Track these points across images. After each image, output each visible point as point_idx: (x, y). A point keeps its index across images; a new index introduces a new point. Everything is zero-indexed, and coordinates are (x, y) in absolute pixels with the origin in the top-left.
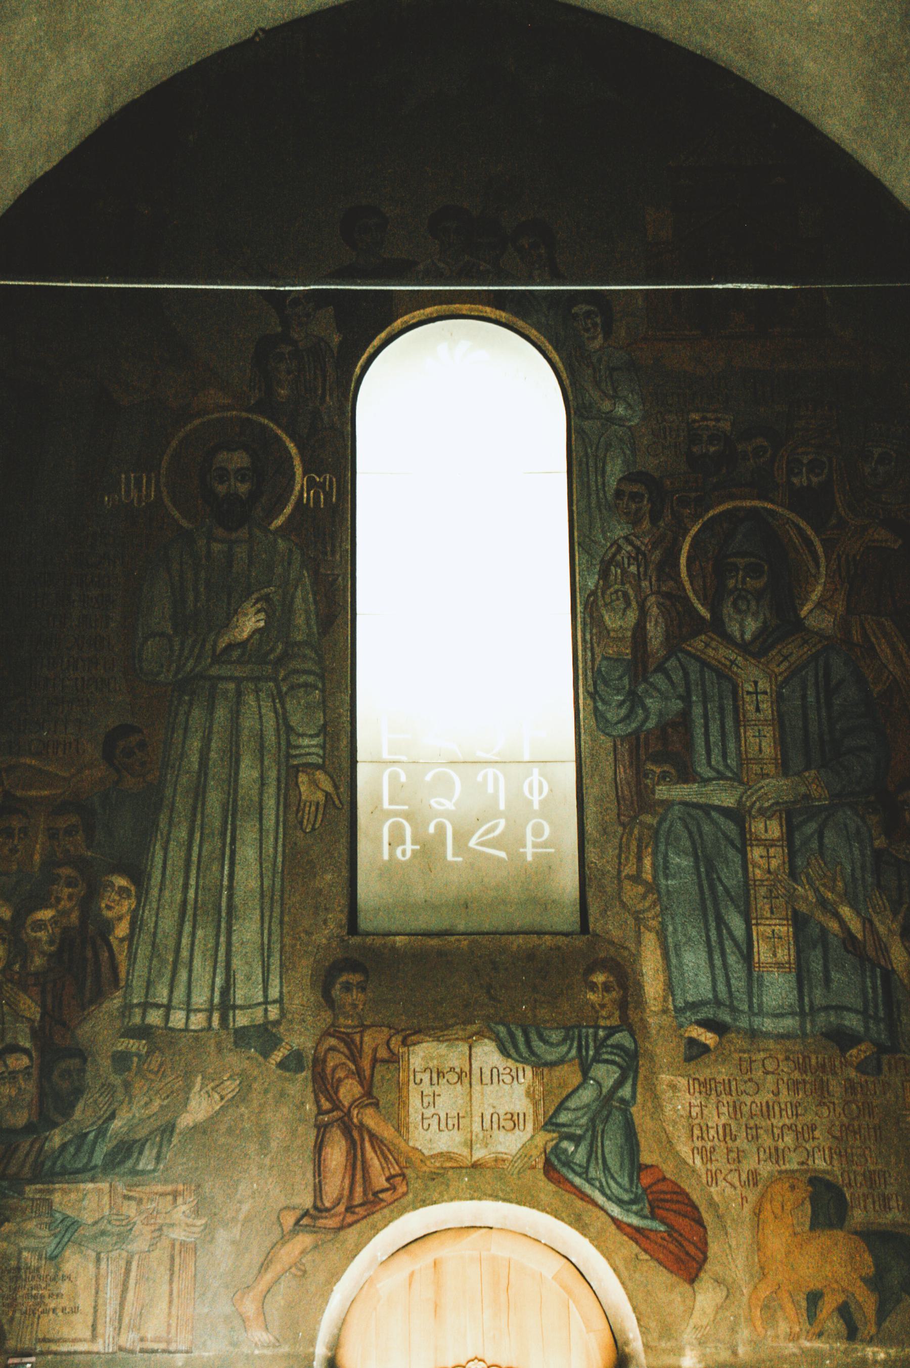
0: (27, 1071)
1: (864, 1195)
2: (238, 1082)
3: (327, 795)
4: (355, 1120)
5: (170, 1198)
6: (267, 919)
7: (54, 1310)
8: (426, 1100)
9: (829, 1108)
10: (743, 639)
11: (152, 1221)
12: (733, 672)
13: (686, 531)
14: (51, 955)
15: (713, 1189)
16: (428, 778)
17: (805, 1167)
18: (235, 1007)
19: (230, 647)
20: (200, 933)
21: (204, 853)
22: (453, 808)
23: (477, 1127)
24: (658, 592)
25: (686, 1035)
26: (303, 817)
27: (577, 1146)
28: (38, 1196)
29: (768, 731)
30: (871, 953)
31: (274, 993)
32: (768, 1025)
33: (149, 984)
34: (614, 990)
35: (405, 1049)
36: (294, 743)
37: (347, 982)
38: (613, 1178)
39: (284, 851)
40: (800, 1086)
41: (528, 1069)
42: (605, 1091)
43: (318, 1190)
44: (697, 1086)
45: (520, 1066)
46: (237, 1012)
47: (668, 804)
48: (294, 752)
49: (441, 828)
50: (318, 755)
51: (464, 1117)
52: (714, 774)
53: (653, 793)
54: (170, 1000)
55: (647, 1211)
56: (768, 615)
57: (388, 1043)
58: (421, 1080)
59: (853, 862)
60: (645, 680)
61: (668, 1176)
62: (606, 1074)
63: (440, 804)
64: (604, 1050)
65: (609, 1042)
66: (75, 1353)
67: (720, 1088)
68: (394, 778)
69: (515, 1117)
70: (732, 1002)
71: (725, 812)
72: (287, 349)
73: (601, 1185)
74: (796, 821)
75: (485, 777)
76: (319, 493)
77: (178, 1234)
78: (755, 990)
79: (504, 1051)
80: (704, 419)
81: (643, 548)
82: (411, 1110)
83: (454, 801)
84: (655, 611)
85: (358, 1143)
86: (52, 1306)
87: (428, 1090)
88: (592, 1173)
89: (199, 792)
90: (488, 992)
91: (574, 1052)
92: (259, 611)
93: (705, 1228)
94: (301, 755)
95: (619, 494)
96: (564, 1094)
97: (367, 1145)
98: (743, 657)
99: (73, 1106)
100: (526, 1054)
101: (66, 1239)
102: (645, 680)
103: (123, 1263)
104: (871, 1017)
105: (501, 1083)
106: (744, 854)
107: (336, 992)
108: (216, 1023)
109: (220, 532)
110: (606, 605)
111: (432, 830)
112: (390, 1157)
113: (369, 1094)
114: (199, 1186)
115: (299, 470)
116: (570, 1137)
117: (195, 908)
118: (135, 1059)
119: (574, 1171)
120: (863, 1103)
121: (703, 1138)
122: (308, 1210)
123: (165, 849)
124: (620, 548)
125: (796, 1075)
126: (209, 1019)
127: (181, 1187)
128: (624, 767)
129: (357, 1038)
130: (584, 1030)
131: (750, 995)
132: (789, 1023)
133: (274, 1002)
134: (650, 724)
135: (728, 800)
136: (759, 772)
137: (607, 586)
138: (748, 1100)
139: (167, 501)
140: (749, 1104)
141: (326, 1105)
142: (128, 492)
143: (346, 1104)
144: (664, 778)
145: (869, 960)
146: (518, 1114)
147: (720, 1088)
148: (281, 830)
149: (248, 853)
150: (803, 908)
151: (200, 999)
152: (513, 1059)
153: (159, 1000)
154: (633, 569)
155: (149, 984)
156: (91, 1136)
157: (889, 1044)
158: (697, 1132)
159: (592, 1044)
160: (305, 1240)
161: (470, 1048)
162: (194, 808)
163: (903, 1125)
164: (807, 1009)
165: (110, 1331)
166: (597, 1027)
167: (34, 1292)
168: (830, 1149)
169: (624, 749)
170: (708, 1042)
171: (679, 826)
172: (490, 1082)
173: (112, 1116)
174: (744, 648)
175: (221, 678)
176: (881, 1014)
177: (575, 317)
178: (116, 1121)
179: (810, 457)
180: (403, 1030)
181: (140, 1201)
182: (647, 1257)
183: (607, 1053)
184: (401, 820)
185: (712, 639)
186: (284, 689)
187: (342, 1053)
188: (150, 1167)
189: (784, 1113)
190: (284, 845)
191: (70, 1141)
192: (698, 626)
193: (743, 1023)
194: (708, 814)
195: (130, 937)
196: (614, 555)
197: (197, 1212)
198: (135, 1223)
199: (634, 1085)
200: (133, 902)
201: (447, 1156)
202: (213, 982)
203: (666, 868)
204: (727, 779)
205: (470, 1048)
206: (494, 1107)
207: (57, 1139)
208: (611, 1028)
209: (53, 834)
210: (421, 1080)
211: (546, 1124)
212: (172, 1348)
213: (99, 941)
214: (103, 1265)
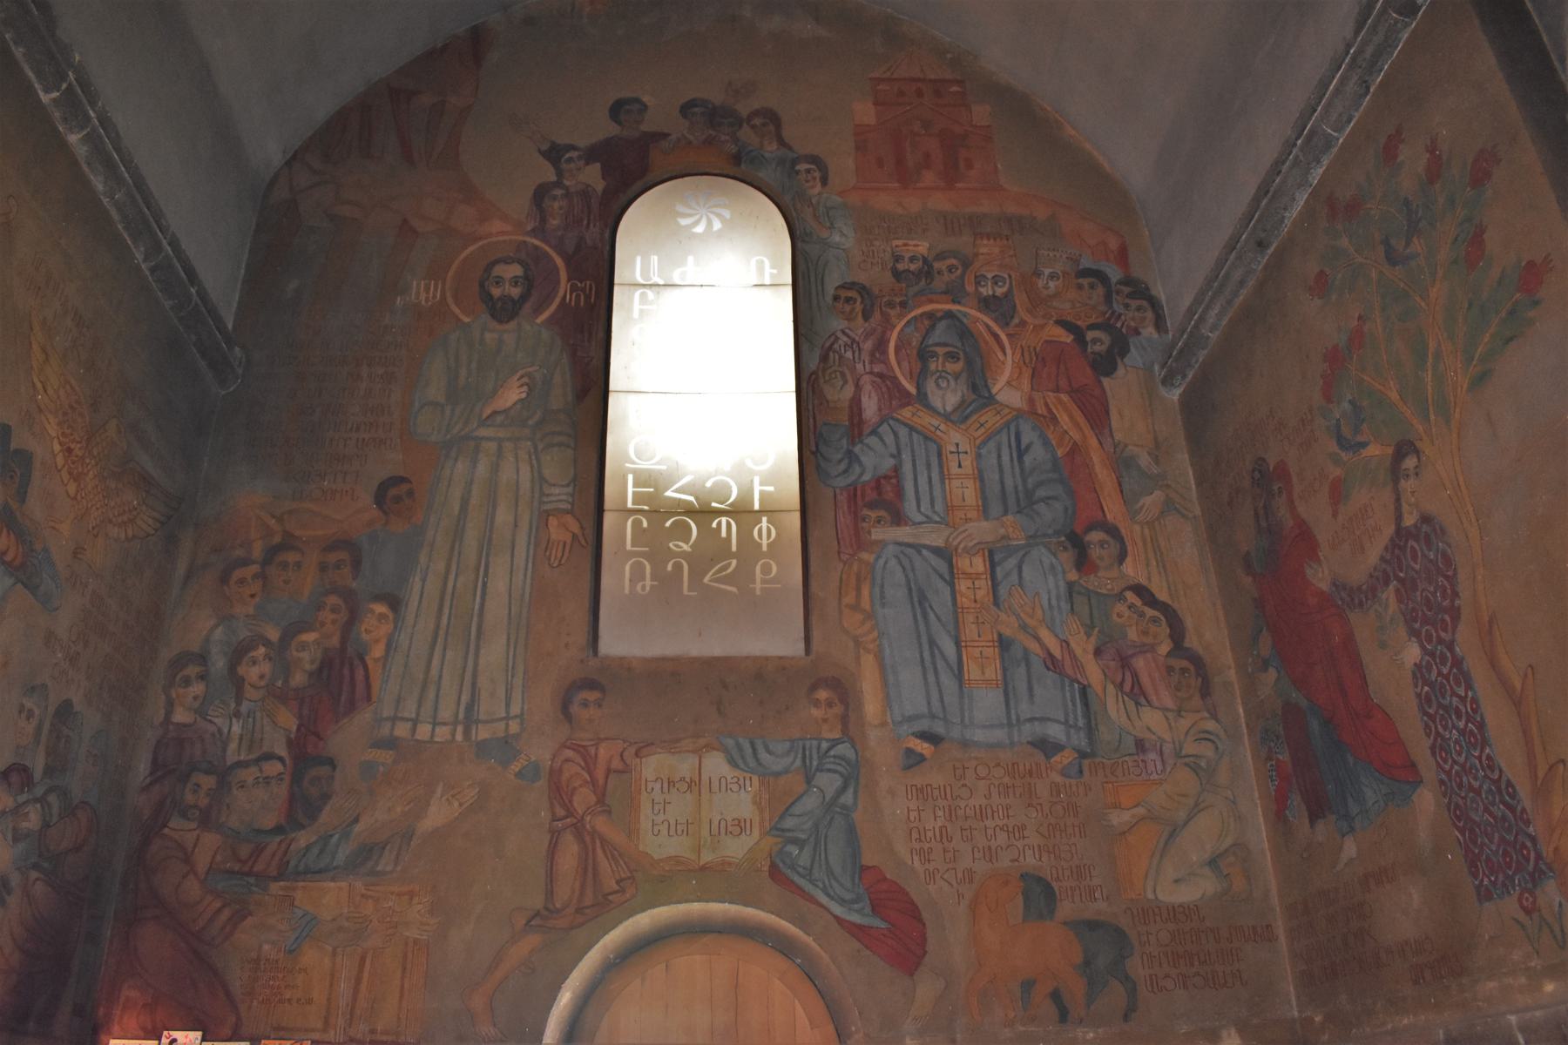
0: (280, 776)
1: (1071, 887)
2: (477, 790)
3: (574, 536)
4: (588, 826)
6: (512, 641)
8: (656, 807)
9: (1037, 811)
10: (945, 410)
11: (388, 919)
12: (937, 436)
13: (895, 327)
14: (311, 674)
15: (930, 887)
16: (668, 524)
17: (1016, 863)
18: (478, 721)
19: (495, 413)
20: (450, 654)
21: (458, 585)
22: (690, 550)
23: (705, 833)
24: (871, 373)
25: (904, 746)
26: (550, 555)
27: (801, 850)
28: (281, 893)
29: (970, 483)
30: (1069, 671)
31: (515, 709)
32: (979, 735)
33: (399, 700)
34: (836, 705)
35: (638, 760)
36: (547, 492)
37: (586, 700)
38: (835, 879)
39: (532, 584)
40: (1011, 790)
41: (755, 779)
42: (827, 799)
43: (550, 893)
44: (914, 791)
45: (748, 775)
46: (479, 725)
47: (882, 544)
48: (545, 499)
49: (678, 567)
50: (569, 502)
51: (692, 823)
52: (924, 519)
53: (869, 533)
54: (418, 714)
55: (868, 910)
56: (965, 391)
57: (622, 756)
58: (653, 789)
59: (1049, 593)
60: (861, 442)
61: (888, 877)
62: (828, 783)
63: (677, 546)
64: (828, 760)
65: (832, 753)
67: (936, 793)
68: (637, 524)
69: (743, 824)
70: (945, 716)
71: (937, 551)
72: (559, 192)
73: (825, 886)
74: (997, 558)
75: (719, 524)
76: (580, 295)
78: (966, 707)
79: (732, 763)
80: (905, 245)
81: (857, 339)
82: (642, 817)
83: (690, 544)
84: (868, 387)
85: (590, 848)
86: (288, 997)
87: (658, 797)
88: (816, 874)
89: (458, 533)
90: (719, 709)
91: (798, 763)
92: (522, 386)
93: (924, 925)
94: (550, 502)
95: (836, 298)
96: (791, 801)
97: (599, 851)
98: (945, 423)
100: (752, 763)
101: (304, 934)
102: (861, 442)
104: (1071, 726)
105: (729, 791)
106: (952, 585)
107: (575, 709)
108: (459, 737)
109: (493, 324)
110: (825, 382)
111: (669, 568)
112: (621, 862)
113: (601, 800)
115: (563, 275)
116: (794, 841)
117: (447, 633)
118: (381, 769)
119: (798, 873)
120: (1068, 805)
121: (921, 841)
122: (539, 911)
123: (424, 580)
124: (837, 339)
125: (1006, 780)
126: (453, 735)
128: (843, 513)
129: (593, 751)
130: (808, 743)
131: (962, 710)
132: (999, 735)
133: (516, 717)
134: (866, 477)
135: (935, 537)
136: (963, 517)
137: (824, 371)
138: (963, 804)
139: (450, 300)
140: (963, 807)
141: (560, 812)
142: (418, 294)
143: (580, 812)
144: (879, 522)
145: (1068, 677)
146: (745, 820)
147: (936, 793)
148: (530, 565)
149: (499, 584)
150: (1007, 632)
151: (446, 713)
152: (742, 769)
153: (406, 715)
154: (849, 354)
155: (399, 700)
156: (337, 836)
157: (1089, 750)
158: (915, 835)
159: (815, 756)
160: (533, 940)
161: (700, 758)
162: (452, 548)
163: (1105, 823)
164: (1014, 722)
166: (820, 740)
167: (271, 983)
168: (1039, 846)
169: (842, 498)
170: (924, 752)
171: (893, 562)
172: (718, 791)
173: (356, 820)
174: (947, 417)
175: (482, 438)
176: (1081, 723)
177: (798, 172)
178: (359, 825)
179: (993, 275)
180: (636, 743)
182: (868, 952)
183: (830, 763)
184: (642, 559)
185: (918, 410)
186: (540, 446)
187: (581, 766)
188: (389, 868)
189: (996, 814)
190: (532, 579)
191: (315, 842)
192: (905, 399)
193: (955, 733)
194: (919, 552)
196: (833, 344)
198: (371, 921)
199: (856, 792)
201: (676, 860)
202: (459, 698)
203: (882, 597)
204: (936, 522)
205: (700, 758)
206: (722, 814)
207: (303, 839)
208: (833, 740)
209: (323, 568)
210: (653, 789)
211: (771, 830)
213: (356, 662)
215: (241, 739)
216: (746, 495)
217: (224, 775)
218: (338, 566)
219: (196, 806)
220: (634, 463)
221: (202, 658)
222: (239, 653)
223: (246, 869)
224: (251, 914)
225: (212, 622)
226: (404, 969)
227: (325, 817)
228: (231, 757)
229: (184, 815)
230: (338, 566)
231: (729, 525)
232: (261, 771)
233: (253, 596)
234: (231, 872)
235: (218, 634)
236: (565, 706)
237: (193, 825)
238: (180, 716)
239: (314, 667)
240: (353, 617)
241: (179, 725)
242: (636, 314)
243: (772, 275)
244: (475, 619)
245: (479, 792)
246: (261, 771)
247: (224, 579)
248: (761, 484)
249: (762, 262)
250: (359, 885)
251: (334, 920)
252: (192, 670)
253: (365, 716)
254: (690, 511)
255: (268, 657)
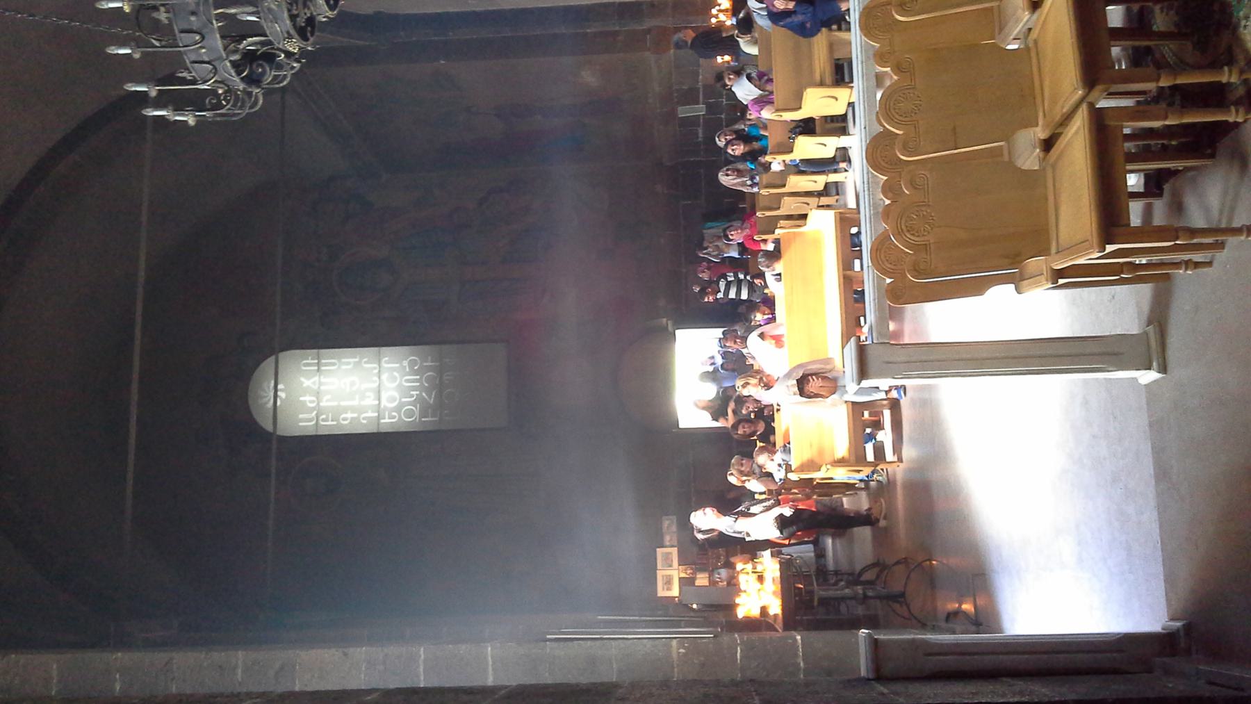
75: (447, 380)
216: (429, 369)
220: (416, 419)
231: (448, 375)
242: (335, 423)
243: (312, 359)
248: (426, 362)
249: (304, 364)
254: (440, 394)
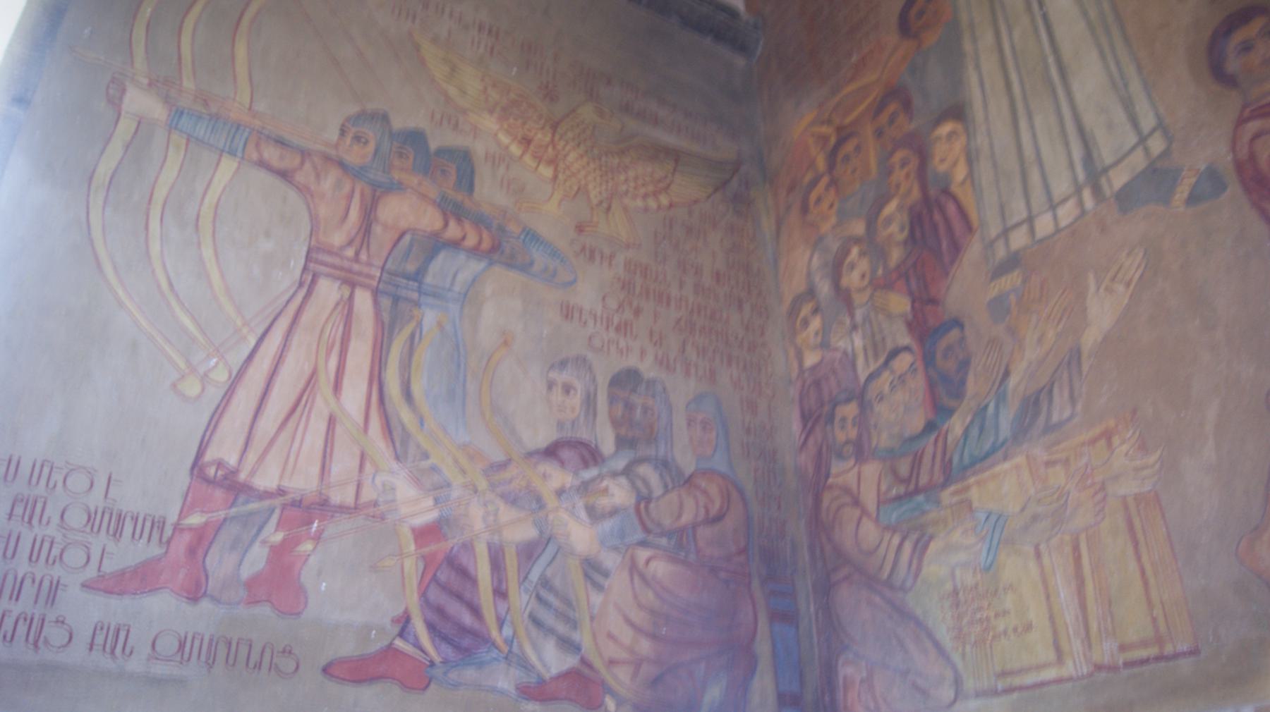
2: (1141, 254)
5: (1103, 442)
7: (1005, 633)
14: (905, 243)
18: (1105, 170)
20: (1038, 120)
28: (955, 499)
31: (1148, 122)
66: (1042, 684)
77: (1128, 488)
86: (1001, 627)
99: (963, 382)
101: (995, 542)
103: (1068, 549)
107: (1233, 65)
114: (1134, 412)
123: (978, 67)
126: (1081, 203)
127: (1112, 423)
151: (1061, 186)
153: (1015, 220)
165: (1077, 646)
167: (978, 616)
173: (1007, 374)
181: (1066, 462)
188: (1067, 414)
191: (972, 422)
195: (971, 174)
197: (1143, 447)
198: (1069, 493)
200: (963, 139)
207: (956, 425)
209: (879, 133)
212: (1169, 649)
214: (1046, 560)
215: (865, 350)
217: (860, 397)
218: (892, 120)
219: (847, 442)
221: (811, 292)
222: (837, 268)
223: (912, 487)
224: (931, 538)
225: (808, 254)
226: (1136, 544)
227: (971, 386)
228: (863, 377)
229: (840, 456)
230: (892, 120)
232: (893, 372)
233: (831, 206)
234: (899, 498)
235: (816, 261)
236: (1219, 73)
237: (852, 462)
238: (811, 359)
239: (906, 232)
240: (923, 156)
241: (814, 368)
244: (1051, 60)
245: (1145, 254)
246: (893, 372)
247: (805, 209)
250: (1040, 453)
251: (1023, 510)
252: (806, 310)
253: (973, 251)
255: (862, 254)
